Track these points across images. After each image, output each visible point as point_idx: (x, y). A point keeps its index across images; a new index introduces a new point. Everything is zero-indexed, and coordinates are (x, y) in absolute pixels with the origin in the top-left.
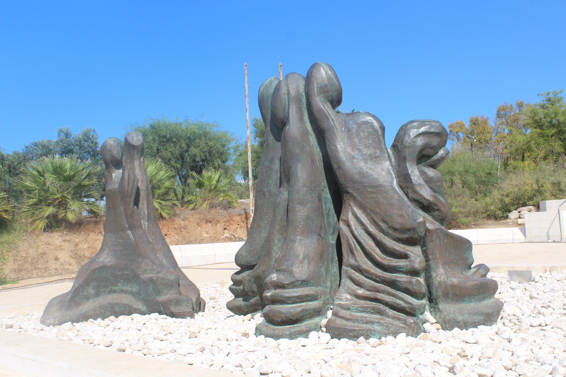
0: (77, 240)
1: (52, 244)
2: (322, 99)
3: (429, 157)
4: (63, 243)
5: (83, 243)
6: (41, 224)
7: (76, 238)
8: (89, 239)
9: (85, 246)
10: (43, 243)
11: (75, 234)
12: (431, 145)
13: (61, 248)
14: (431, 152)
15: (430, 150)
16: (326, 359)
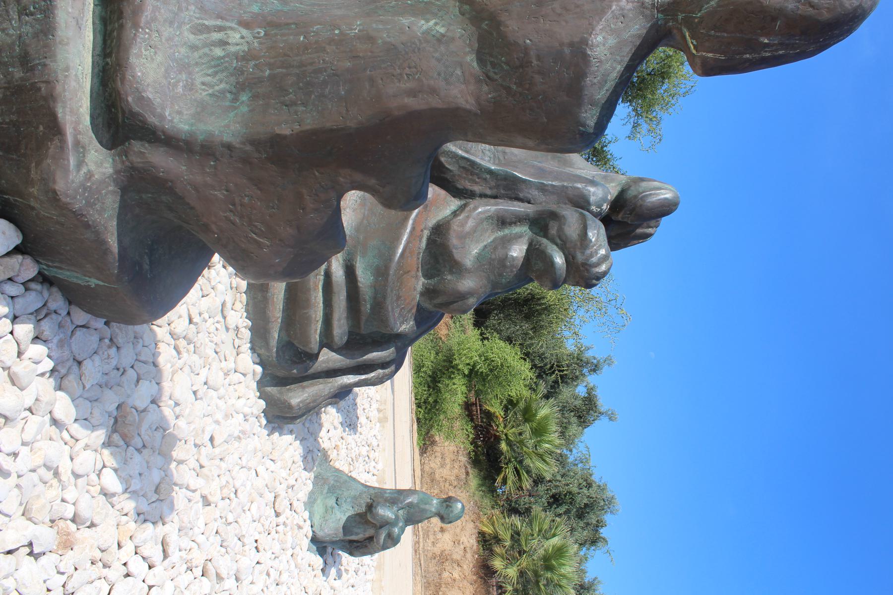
0: (465, 567)
1: (462, 532)
2: (624, 181)
3: (546, 236)
4: (462, 547)
5: (461, 574)
6: (488, 530)
7: (469, 564)
8: (465, 582)
9: (456, 575)
10: (464, 524)
11: (474, 567)
12: (564, 225)
13: (456, 542)
14: (553, 231)
15: (556, 228)
16: (224, 574)
